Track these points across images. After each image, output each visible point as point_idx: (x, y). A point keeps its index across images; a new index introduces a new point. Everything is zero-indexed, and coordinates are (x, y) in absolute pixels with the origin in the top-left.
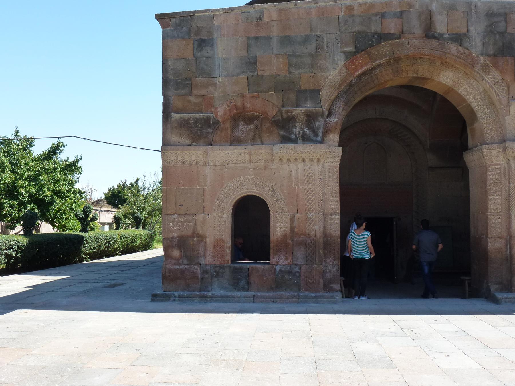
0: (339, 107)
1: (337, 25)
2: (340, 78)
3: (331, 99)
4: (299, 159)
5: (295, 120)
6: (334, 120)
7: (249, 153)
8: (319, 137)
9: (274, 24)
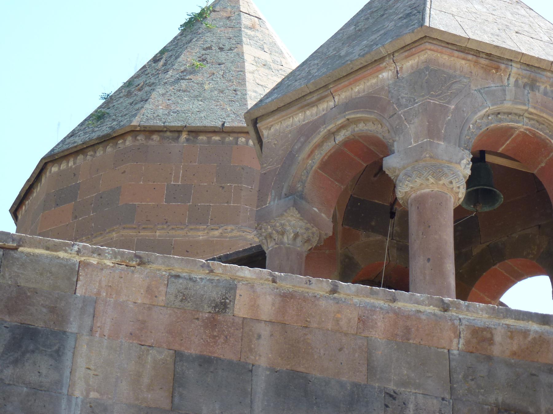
1: (446, 374)
9: (265, 330)
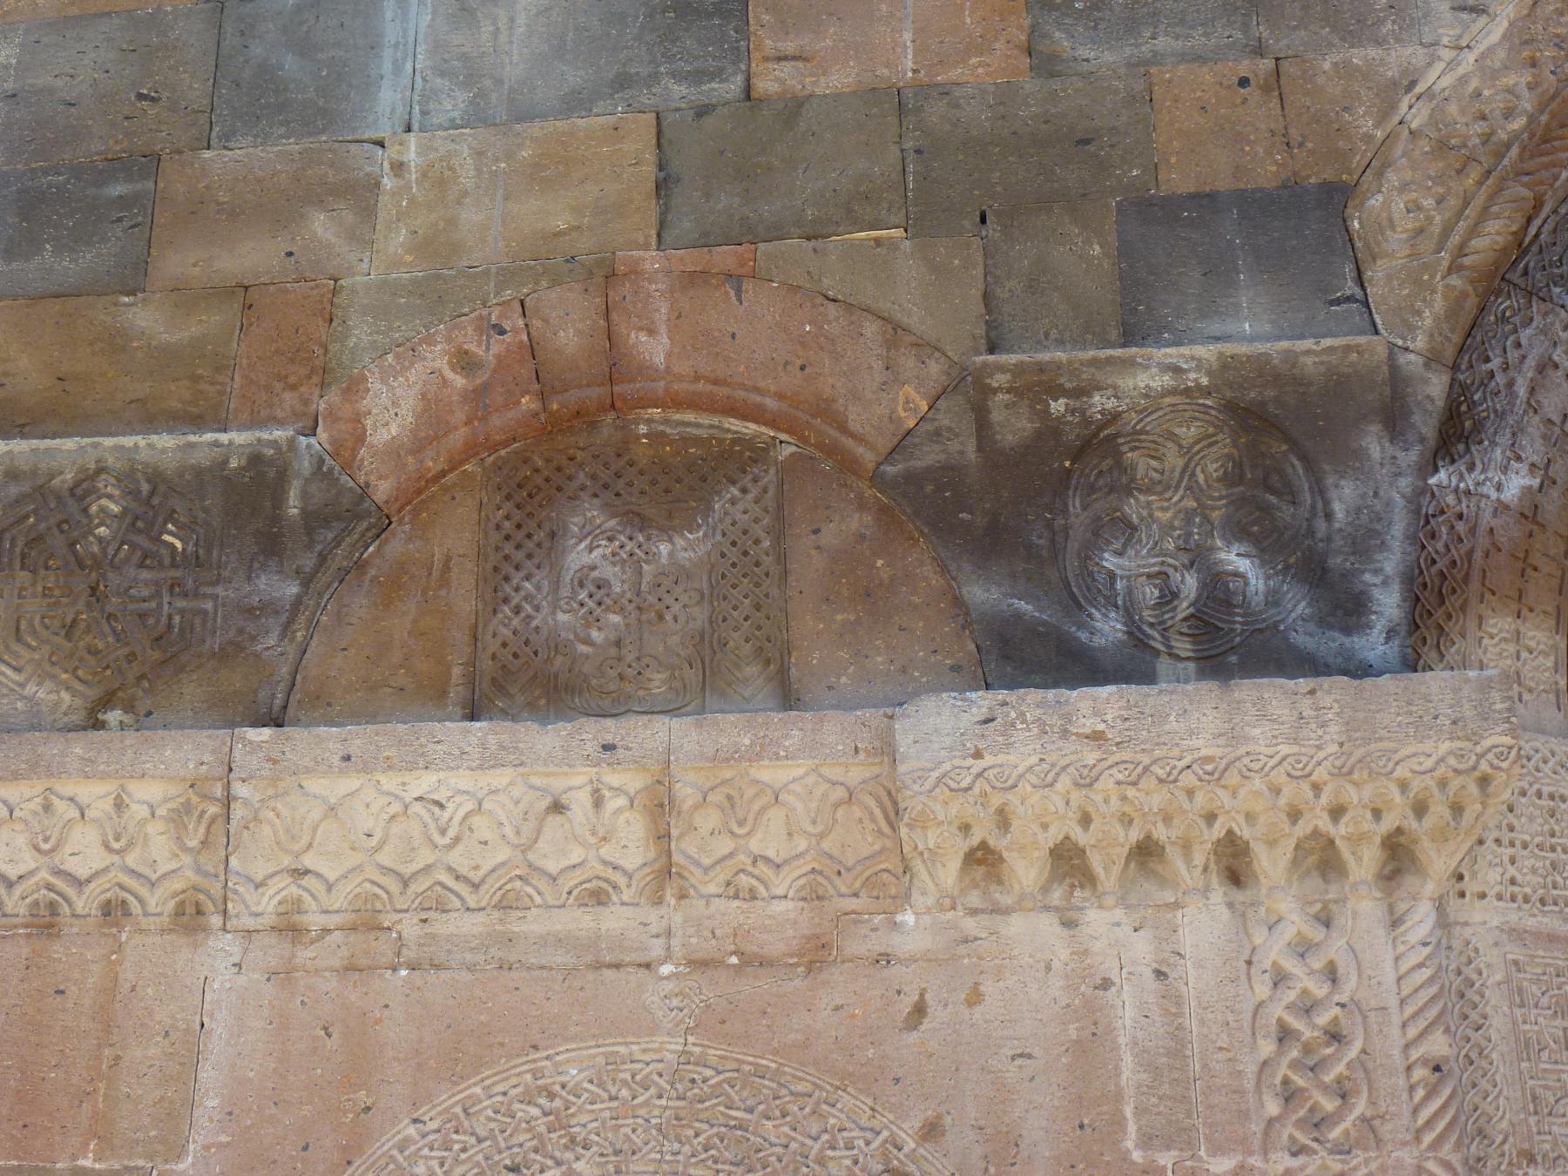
0: (1541, 369)
2: (1530, 87)
3: (1467, 261)
4: (1186, 847)
5: (1120, 466)
6: (1499, 487)
7: (646, 788)
8: (1377, 634)
